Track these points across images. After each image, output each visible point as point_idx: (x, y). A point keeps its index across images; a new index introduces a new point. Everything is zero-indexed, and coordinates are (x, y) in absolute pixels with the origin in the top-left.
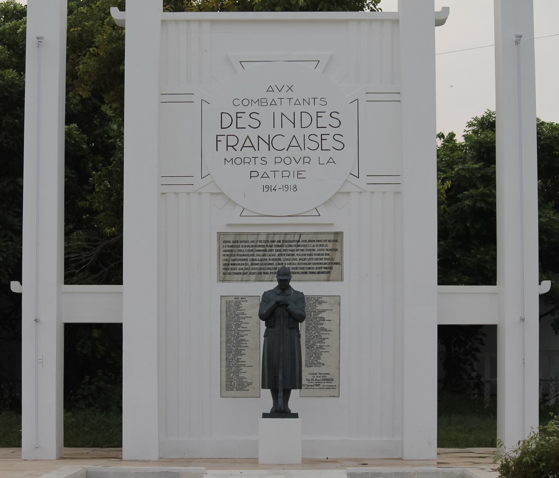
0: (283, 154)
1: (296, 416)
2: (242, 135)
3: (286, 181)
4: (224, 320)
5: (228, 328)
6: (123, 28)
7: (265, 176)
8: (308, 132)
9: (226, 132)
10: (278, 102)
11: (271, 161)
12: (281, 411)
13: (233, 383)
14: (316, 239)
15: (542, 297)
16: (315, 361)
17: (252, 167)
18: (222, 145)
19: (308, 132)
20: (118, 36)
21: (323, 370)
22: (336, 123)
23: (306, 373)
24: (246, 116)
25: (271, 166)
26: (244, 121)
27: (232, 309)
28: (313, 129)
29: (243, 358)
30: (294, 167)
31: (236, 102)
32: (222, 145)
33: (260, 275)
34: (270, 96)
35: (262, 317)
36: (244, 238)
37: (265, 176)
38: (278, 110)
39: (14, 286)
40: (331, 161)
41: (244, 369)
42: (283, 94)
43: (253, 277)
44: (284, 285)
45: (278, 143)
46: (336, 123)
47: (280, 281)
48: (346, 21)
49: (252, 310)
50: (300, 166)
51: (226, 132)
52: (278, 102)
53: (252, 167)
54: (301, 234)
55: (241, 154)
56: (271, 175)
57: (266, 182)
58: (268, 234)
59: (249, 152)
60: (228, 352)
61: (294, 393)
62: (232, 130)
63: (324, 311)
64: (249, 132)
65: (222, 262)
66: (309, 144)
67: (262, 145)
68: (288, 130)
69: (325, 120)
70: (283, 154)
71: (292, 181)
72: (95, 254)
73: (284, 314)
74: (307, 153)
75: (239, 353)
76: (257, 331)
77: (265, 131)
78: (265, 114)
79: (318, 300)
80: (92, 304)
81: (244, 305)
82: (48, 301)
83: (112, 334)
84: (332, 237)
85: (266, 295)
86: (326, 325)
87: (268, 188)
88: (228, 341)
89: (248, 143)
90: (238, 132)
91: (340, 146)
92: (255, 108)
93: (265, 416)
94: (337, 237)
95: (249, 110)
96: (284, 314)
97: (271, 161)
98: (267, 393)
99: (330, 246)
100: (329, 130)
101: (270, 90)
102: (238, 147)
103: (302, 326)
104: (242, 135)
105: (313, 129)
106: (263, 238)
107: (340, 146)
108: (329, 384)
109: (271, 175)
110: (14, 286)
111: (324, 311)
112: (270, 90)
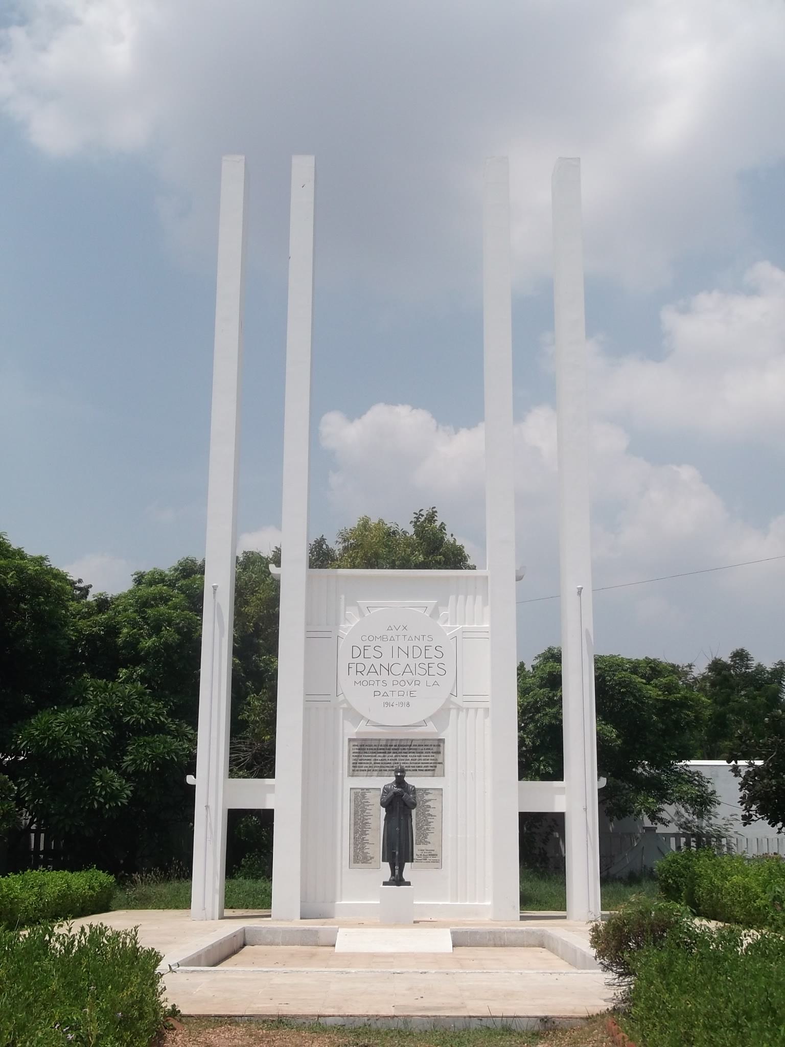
0: (399, 678)
1: (408, 884)
4: (353, 807)
5: (356, 813)
6: (279, 581)
7: (386, 694)
8: (418, 661)
9: (356, 661)
12: (397, 880)
13: (360, 857)
15: (601, 791)
17: (375, 688)
18: (353, 671)
19: (418, 661)
20: (276, 585)
21: (429, 847)
23: (417, 850)
26: (370, 652)
27: (359, 797)
28: (422, 659)
29: (367, 837)
32: (353, 671)
33: (381, 771)
35: (382, 804)
36: (369, 743)
37: (386, 694)
39: (190, 779)
40: (436, 683)
41: (367, 846)
43: (375, 773)
44: (400, 782)
45: (397, 669)
47: (397, 776)
48: (448, 578)
50: (413, 687)
51: (356, 661)
53: (375, 688)
54: (412, 740)
55: (367, 678)
56: (390, 694)
57: (385, 699)
58: (387, 740)
59: (373, 676)
60: (356, 833)
61: (407, 865)
63: (430, 800)
64: (373, 661)
65: (352, 761)
66: (419, 670)
67: (384, 671)
68: (404, 660)
69: (431, 652)
70: (399, 678)
71: (405, 699)
72: (253, 753)
74: (418, 677)
75: (364, 833)
79: (426, 791)
80: (251, 794)
81: (368, 795)
82: (215, 790)
83: (267, 817)
84: (436, 743)
85: (386, 790)
86: (431, 811)
89: (372, 670)
90: (364, 661)
91: (442, 672)
92: (378, 642)
93: (385, 884)
95: (373, 644)
98: (387, 865)
99: (435, 749)
100: (434, 660)
102: (365, 673)
103: (414, 812)
106: (384, 743)
107: (442, 672)
108: (434, 858)
109: (390, 694)
110: (190, 779)
111: (430, 800)
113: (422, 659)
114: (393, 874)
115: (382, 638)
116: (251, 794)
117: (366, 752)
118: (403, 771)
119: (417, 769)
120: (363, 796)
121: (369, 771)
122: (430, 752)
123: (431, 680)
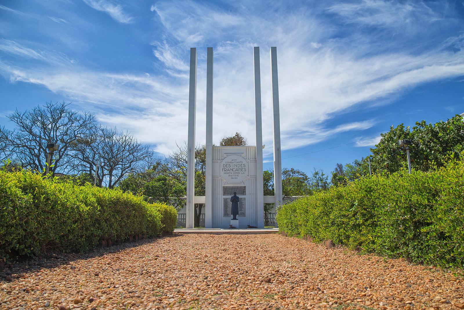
1: (237, 220)
2: (227, 168)
5: (225, 204)
12: (235, 218)
13: (226, 214)
14: (241, 187)
16: (241, 210)
21: (242, 212)
25: (233, 174)
27: (225, 201)
30: (237, 174)
34: (232, 161)
38: (234, 164)
40: (244, 173)
44: (235, 196)
45: (234, 170)
49: (229, 201)
50: (238, 174)
57: (232, 177)
59: (228, 171)
60: (225, 208)
62: (225, 167)
73: (235, 200)
75: (227, 209)
76: (230, 204)
78: (231, 164)
79: (241, 199)
80: (201, 200)
86: (243, 203)
88: (225, 206)
93: (232, 220)
94: (245, 187)
96: (235, 200)
100: (243, 167)
101: (232, 160)
103: (238, 203)
104: (227, 168)
105: (240, 167)
108: (244, 214)
112: (232, 160)
114: (234, 217)
116: (201, 200)
117: (226, 190)
118: (235, 193)
119: (240, 194)
120: (227, 200)
121: (228, 194)
122: (243, 190)
123: (242, 172)
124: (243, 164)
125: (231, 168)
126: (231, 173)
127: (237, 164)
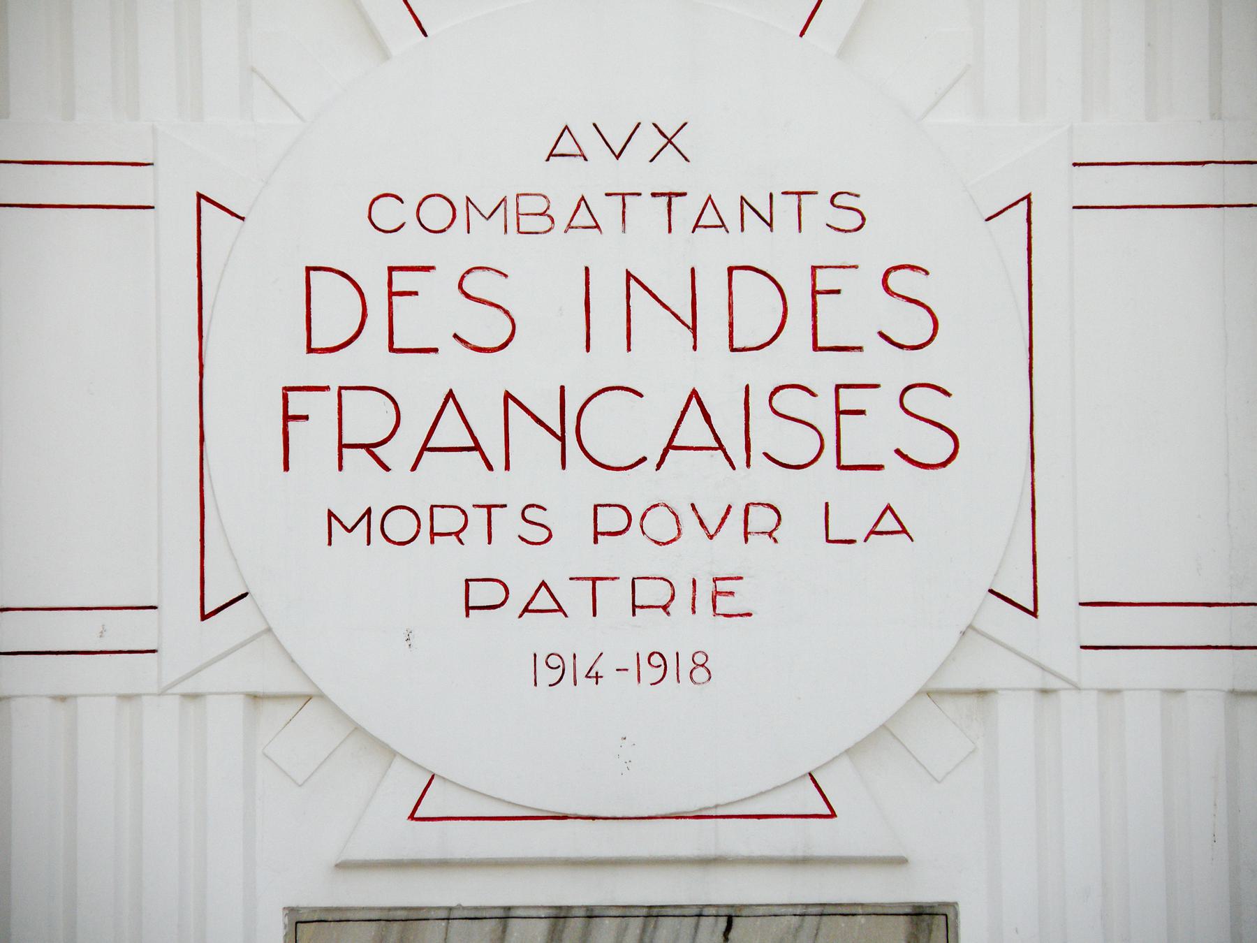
3: (654, 632)
10: (608, 211)
11: (571, 525)
18: (315, 439)
22: (913, 326)
24: (881, 404)
28: (792, 358)
30: (694, 559)
31: (387, 213)
34: (563, 184)
42: (636, 171)
46: (913, 326)
52: (608, 211)
53: (474, 556)
56: (575, 597)
57: (545, 633)
62: (368, 363)
68: (665, 363)
70: (636, 490)
77: (537, 370)
87: (559, 668)
97: (571, 525)
100: (880, 364)
109: (575, 597)
113: (792, 358)
115: (519, 214)
123: (857, 501)
124: (873, 252)
125: (503, 372)
126: (537, 527)
127: (713, 253)
